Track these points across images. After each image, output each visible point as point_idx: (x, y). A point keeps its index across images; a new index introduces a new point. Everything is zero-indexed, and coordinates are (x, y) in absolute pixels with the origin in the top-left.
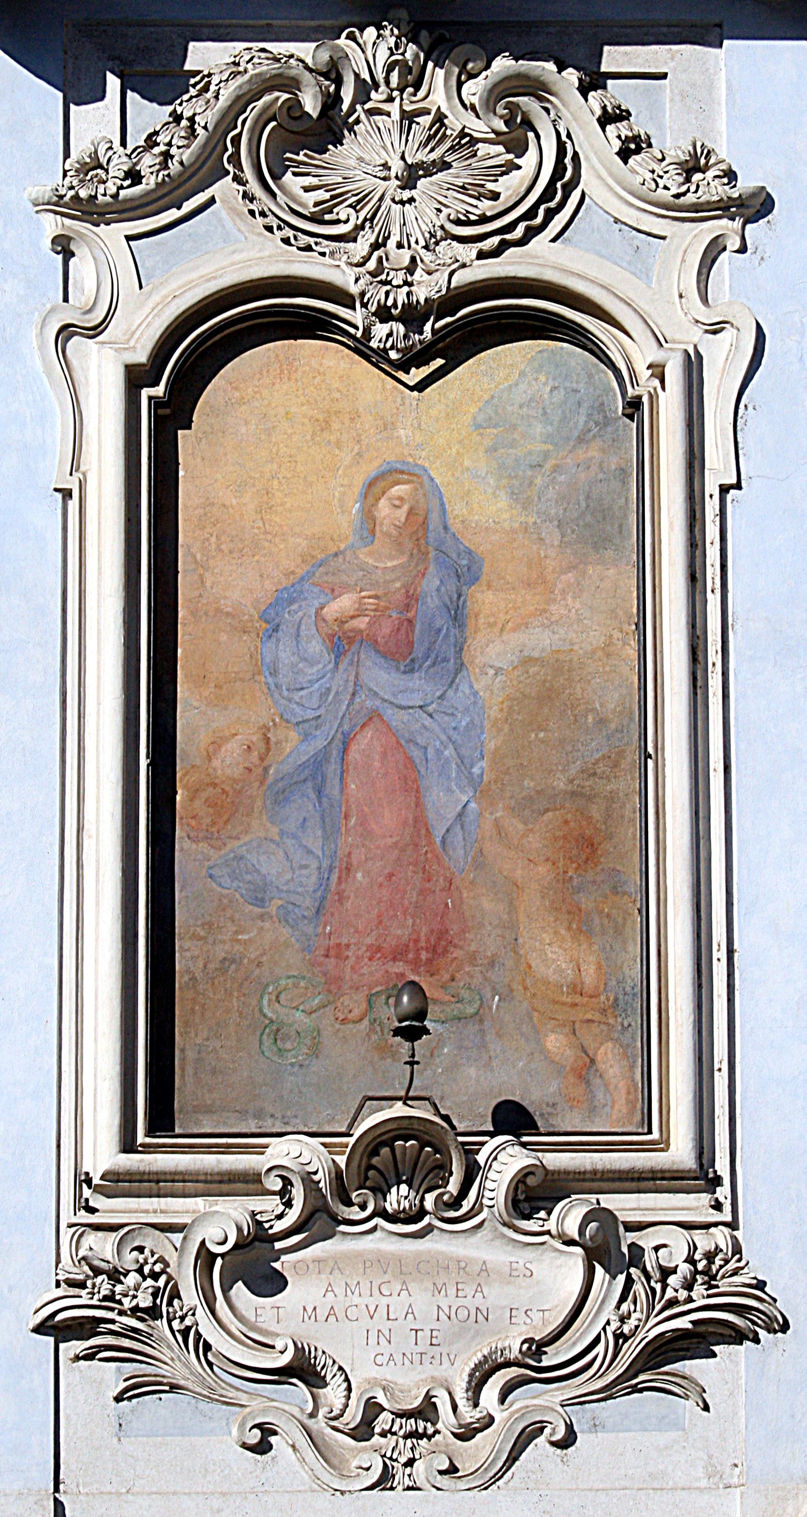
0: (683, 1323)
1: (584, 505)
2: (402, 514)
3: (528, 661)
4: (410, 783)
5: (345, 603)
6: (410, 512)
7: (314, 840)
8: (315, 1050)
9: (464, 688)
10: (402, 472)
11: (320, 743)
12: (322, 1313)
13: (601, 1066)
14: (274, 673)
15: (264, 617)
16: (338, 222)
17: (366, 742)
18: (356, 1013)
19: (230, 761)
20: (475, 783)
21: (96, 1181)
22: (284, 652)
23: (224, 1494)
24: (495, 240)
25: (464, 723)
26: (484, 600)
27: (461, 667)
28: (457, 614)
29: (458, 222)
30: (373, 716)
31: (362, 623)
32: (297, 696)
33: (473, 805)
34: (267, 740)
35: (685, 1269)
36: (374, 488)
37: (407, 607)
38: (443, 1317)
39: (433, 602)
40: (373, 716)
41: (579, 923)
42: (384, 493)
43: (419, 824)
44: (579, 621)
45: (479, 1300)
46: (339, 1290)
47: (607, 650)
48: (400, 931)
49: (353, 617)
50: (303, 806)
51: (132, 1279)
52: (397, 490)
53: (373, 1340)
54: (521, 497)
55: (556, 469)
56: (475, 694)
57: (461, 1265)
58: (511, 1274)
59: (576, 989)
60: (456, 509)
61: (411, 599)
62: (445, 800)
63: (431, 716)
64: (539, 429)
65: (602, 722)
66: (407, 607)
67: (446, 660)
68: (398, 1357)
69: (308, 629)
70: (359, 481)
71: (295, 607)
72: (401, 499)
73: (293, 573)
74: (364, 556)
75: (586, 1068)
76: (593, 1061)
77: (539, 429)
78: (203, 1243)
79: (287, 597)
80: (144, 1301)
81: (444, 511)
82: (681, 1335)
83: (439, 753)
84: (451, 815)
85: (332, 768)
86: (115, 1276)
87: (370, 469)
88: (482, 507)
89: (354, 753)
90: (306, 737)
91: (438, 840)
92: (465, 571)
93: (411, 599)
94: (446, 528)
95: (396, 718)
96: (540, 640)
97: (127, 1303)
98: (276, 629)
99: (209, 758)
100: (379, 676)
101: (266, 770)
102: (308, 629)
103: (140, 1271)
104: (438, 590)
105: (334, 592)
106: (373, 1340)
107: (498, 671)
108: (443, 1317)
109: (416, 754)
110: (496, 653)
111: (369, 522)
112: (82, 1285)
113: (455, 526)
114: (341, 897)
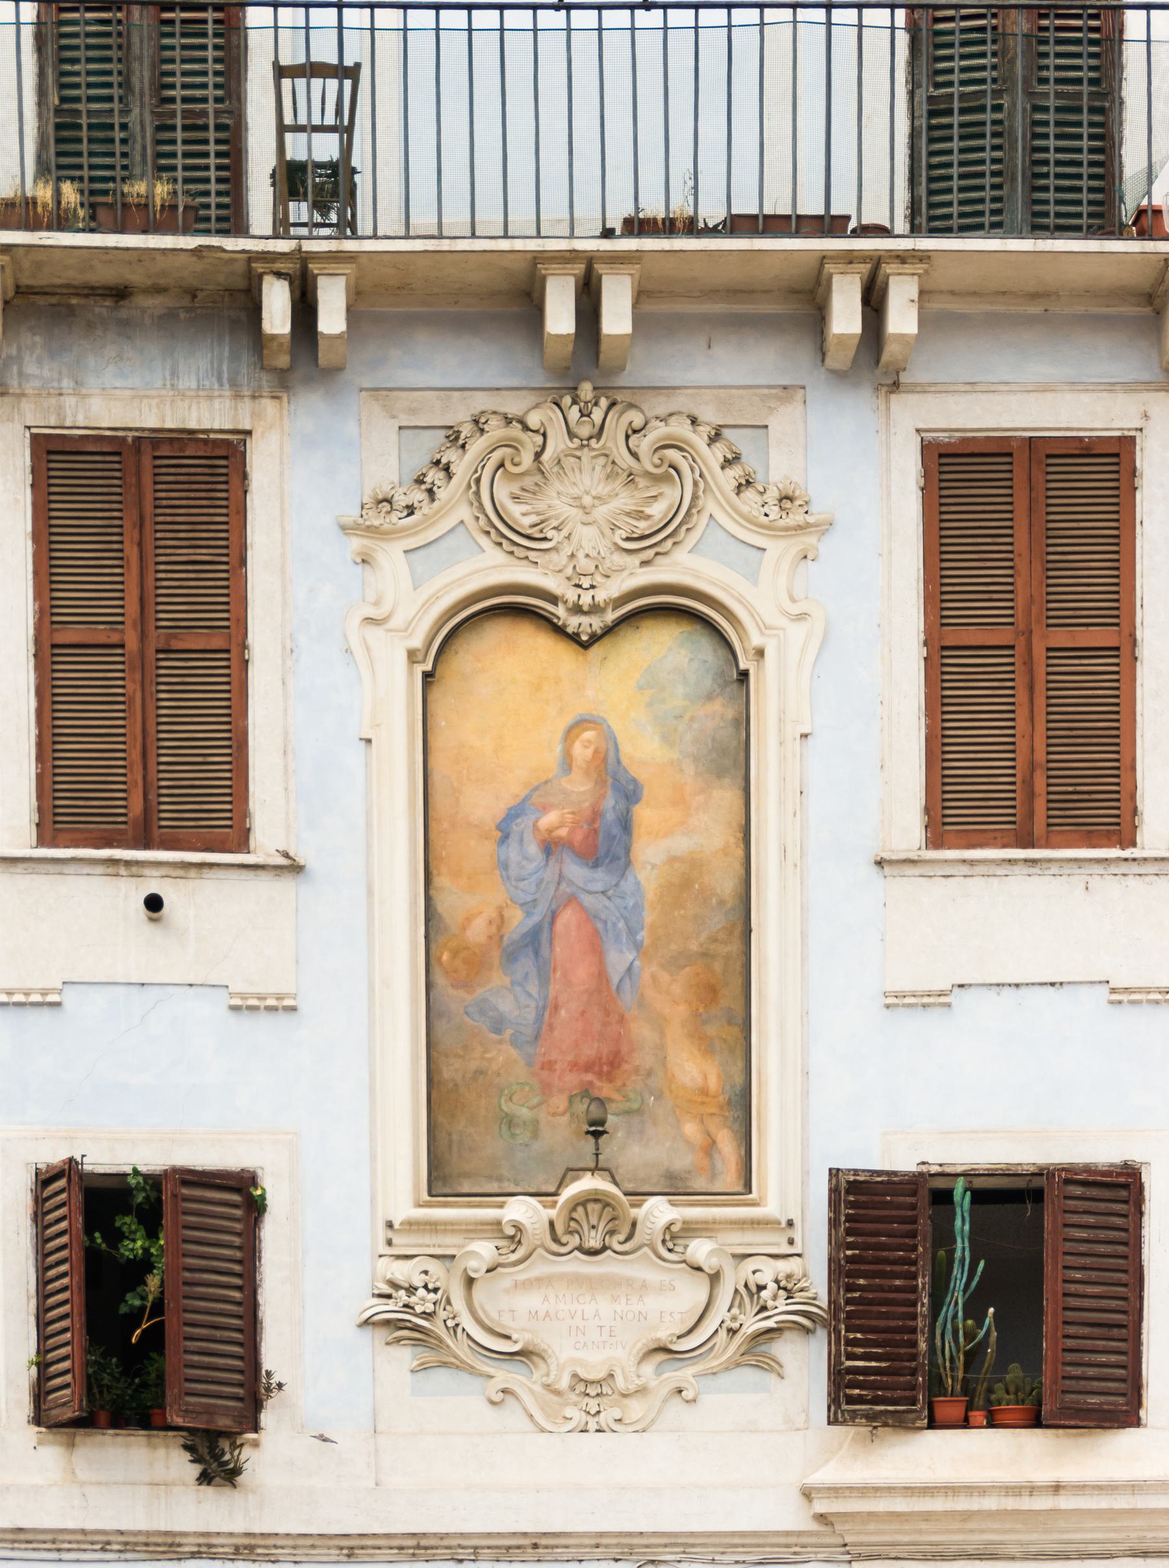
0: (770, 1323)
1: (710, 746)
2: (589, 752)
3: (672, 859)
4: (596, 948)
6: (596, 752)
7: (533, 988)
8: (535, 1135)
9: (630, 879)
10: (589, 722)
11: (536, 919)
12: (541, 1314)
13: (720, 1145)
15: (499, 828)
16: (545, 539)
17: (567, 917)
18: (561, 1109)
19: (477, 932)
20: (638, 946)
21: (396, 1226)
22: (512, 853)
24: (651, 552)
25: (631, 904)
26: (643, 814)
27: (628, 863)
28: (626, 824)
29: (628, 539)
30: (572, 899)
31: (563, 832)
32: (522, 884)
33: (637, 963)
34: (502, 917)
35: (772, 1286)
38: (618, 1317)
39: (610, 816)
40: (572, 899)
41: (707, 1046)
42: (577, 737)
43: (602, 975)
46: (552, 1299)
47: (725, 851)
48: (589, 1051)
49: (557, 828)
50: (526, 964)
51: (421, 1292)
52: (589, 735)
53: (573, 1332)
54: (667, 739)
55: (692, 719)
56: (638, 883)
57: (629, 1282)
58: (662, 1288)
59: (704, 1091)
60: (627, 749)
62: (618, 959)
63: (609, 898)
64: (680, 690)
65: (722, 903)
67: (619, 858)
69: (529, 836)
71: (519, 820)
72: (589, 741)
73: (517, 796)
74: (565, 783)
75: (710, 1147)
76: (714, 1142)
78: (465, 1270)
79: (514, 814)
80: (430, 1308)
82: (770, 1331)
83: (614, 925)
84: (622, 968)
85: (545, 936)
86: (411, 1290)
87: (569, 720)
88: (644, 748)
89: (559, 926)
90: (528, 914)
91: (614, 987)
92: (630, 793)
93: (596, 814)
94: (619, 762)
95: (587, 900)
96: (681, 844)
97: (419, 1309)
99: (464, 929)
100: (576, 871)
101: (502, 937)
102: (529, 836)
103: (426, 1287)
104: (614, 808)
105: (545, 809)
106: (573, 1332)
107: (654, 866)
108: (618, 1317)
109: (600, 926)
110: (653, 853)
112: (389, 1297)
113: (625, 761)
114: (551, 1027)
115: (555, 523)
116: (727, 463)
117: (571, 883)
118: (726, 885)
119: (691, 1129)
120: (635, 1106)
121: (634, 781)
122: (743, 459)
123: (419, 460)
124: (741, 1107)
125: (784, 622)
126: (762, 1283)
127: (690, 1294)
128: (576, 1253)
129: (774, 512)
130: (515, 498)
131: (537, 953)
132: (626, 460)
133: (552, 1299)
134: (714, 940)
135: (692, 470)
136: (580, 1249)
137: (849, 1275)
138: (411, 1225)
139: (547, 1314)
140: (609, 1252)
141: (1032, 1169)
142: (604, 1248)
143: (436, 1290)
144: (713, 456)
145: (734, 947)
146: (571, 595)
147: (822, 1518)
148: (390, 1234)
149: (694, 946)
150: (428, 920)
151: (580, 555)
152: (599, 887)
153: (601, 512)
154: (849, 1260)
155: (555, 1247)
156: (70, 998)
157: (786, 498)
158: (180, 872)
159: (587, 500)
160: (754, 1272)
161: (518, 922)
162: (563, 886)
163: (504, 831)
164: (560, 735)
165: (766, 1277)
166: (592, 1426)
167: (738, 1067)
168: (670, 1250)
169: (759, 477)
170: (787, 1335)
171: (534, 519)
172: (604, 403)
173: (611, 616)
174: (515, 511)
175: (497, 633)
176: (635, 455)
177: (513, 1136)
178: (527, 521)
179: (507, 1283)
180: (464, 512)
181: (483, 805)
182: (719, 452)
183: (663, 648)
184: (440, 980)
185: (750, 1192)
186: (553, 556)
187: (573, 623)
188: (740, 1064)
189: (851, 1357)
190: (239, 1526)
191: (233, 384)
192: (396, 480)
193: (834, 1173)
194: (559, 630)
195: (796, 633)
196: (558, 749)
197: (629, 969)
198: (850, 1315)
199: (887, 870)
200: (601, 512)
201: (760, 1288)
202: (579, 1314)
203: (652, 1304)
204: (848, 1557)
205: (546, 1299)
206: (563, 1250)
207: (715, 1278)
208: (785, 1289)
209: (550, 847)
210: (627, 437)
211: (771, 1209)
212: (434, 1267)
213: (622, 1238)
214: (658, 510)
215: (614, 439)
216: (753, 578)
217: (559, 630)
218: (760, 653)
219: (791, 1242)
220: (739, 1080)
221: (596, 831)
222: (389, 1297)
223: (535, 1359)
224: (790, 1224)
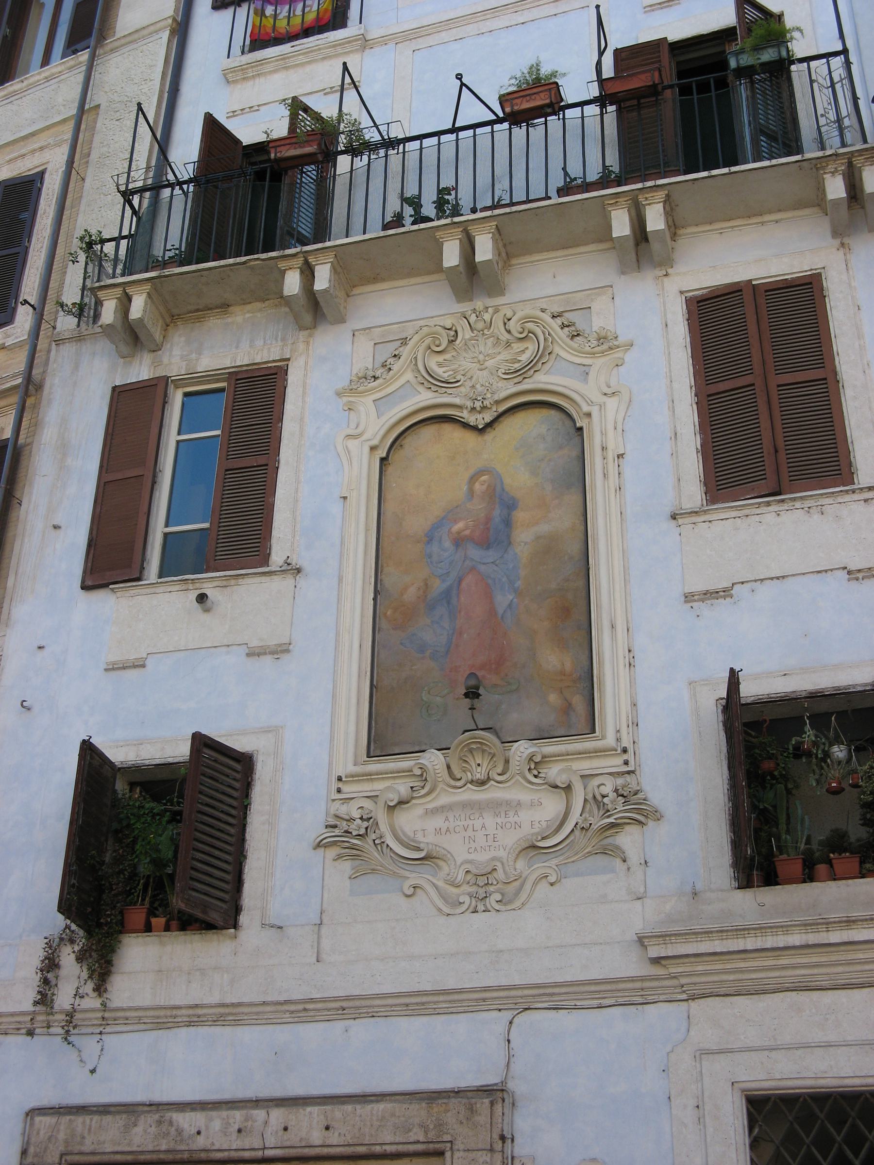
2: (484, 487)
3: (538, 538)
5: (460, 525)
6: (489, 486)
11: (448, 583)
14: (430, 556)
15: (426, 535)
17: (469, 579)
19: (411, 594)
22: (435, 548)
23: (397, 920)
26: (520, 516)
27: (510, 543)
28: (508, 523)
30: (473, 569)
31: (467, 532)
34: (426, 585)
35: (613, 795)
36: (473, 479)
38: (499, 827)
43: (492, 612)
44: (561, 519)
45: (516, 818)
51: (359, 821)
56: (516, 554)
57: (508, 803)
59: (562, 673)
60: (507, 481)
62: (502, 600)
68: (479, 849)
70: (467, 476)
72: (484, 481)
76: (570, 704)
79: (437, 526)
80: (362, 831)
81: (502, 483)
87: (472, 471)
88: (518, 478)
89: (464, 585)
91: (500, 616)
92: (510, 505)
93: (488, 519)
94: (503, 490)
95: (482, 568)
96: (544, 528)
97: (354, 834)
98: (431, 540)
99: (402, 595)
100: (474, 553)
103: (361, 818)
105: (456, 522)
107: (526, 543)
108: (499, 827)
109: (490, 581)
110: (524, 537)
111: (471, 492)
112: (335, 827)
115: (463, 373)
117: (472, 560)
118: (575, 548)
119: (553, 698)
120: (514, 687)
121: (513, 498)
122: (577, 325)
125: (605, 398)
126: (604, 793)
127: (551, 807)
128: (469, 785)
130: (440, 365)
131: (449, 603)
133: (451, 819)
135: (544, 334)
136: (471, 782)
138: (355, 778)
139: (448, 830)
140: (492, 782)
141: (804, 694)
142: (489, 779)
144: (555, 324)
145: (581, 583)
147: (656, 961)
148: (340, 785)
149: (553, 586)
150: (376, 592)
151: (478, 386)
153: (490, 363)
155: (453, 783)
157: (601, 339)
158: (225, 583)
159: (481, 357)
160: (599, 786)
161: (438, 586)
162: (467, 562)
163: (429, 538)
165: (608, 789)
166: (481, 907)
167: (584, 658)
168: (536, 776)
169: (587, 332)
170: (627, 828)
174: (440, 371)
175: (428, 432)
176: (509, 332)
178: (446, 375)
179: (420, 811)
180: (409, 376)
181: (417, 524)
182: (559, 321)
184: (384, 624)
185: (594, 732)
186: (462, 389)
187: (472, 419)
188: (587, 652)
190: (215, 998)
191: (283, 339)
192: (370, 367)
194: (466, 425)
195: (612, 404)
196: (465, 488)
197: (510, 605)
199: (680, 521)
200: (490, 363)
202: (471, 827)
203: (525, 816)
204: (684, 996)
205: (447, 819)
206: (459, 784)
207: (568, 788)
208: (622, 796)
210: (505, 324)
211: (610, 740)
212: (368, 804)
214: (525, 358)
217: (466, 425)
218: (589, 415)
219: (626, 763)
220: (586, 663)
221: (488, 529)
222: (335, 827)
223: (441, 863)
224: (625, 751)
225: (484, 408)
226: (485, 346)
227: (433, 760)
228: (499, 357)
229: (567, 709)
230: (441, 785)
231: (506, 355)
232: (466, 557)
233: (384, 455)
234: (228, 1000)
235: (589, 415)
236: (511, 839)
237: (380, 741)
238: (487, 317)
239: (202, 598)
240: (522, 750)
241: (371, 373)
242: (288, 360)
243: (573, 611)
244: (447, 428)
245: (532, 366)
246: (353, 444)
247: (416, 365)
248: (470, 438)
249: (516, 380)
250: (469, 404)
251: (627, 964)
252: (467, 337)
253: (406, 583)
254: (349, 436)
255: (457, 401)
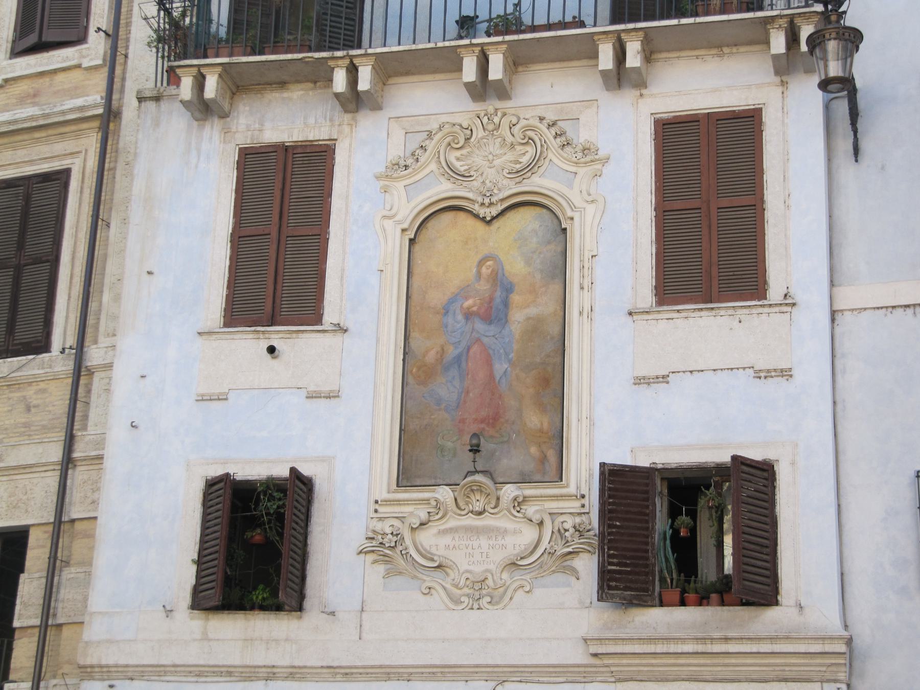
0: (570, 549)
2: (490, 271)
3: (528, 319)
4: (489, 363)
6: (493, 271)
7: (457, 383)
8: (455, 455)
11: (459, 350)
12: (451, 547)
14: (446, 327)
15: (444, 308)
17: (475, 349)
19: (431, 357)
20: (510, 361)
22: (450, 320)
26: (516, 298)
27: (507, 321)
28: (506, 304)
29: (509, 173)
30: (478, 340)
31: (475, 309)
34: (443, 350)
35: (572, 530)
36: (481, 263)
37: (490, 302)
39: (498, 300)
40: (478, 340)
41: (542, 407)
43: (491, 376)
44: (546, 306)
45: (503, 542)
46: (457, 539)
48: (483, 413)
50: (454, 372)
51: (390, 536)
52: (489, 263)
54: (528, 263)
55: (540, 253)
58: (515, 532)
59: (541, 431)
60: (507, 267)
61: (491, 299)
62: (500, 367)
64: (535, 240)
65: (552, 338)
66: (490, 302)
69: (458, 311)
75: (543, 459)
77: (535, 240)
79: (452, 300)
80: (393, 544)
82: (570, 553)
86: (385, 534)
87: (479, 257)
88: (516, 266)
89: (471, 352)
90: (456, 348)
92: (509, 289)
93: (491, 299)
96: (533, 311)
97: (387, 545)
99: (424, 357)
100: (480, 326)
102: (458, 311)
103: (392, 533)
105: (466, 298)
107: (519, 322)
109: (491, 352)
110: (518, 317)
111: (479, 273)
112: (373, 538)
113: (507, 274)
114: (465, 402)
115: (475, 168)
116: (556, 136)
117: (478, 332)
118: (556, 330)
119: (533, 450)
120: (505, 439)
121: (511, 283)
122: (568, 134)
123: (413, 145)
124: (558, 439)
125: (585, 205)
126: (567, 528)
127: (529, 534)
129: (580, 155)
130: (458, 159)
132: (510, 139)
133: (457, 539)
134: (548, 356)
136: (472, 512)
137: (610, 519)
138: (387, 502)
139: (454, 547)
141: (713, 465)
143: (397, 535)
145: (559, 359)
146: (480, 199)
147: (595, 655)
148: (377, 507)
149: (538, 360)
150: (405, 354)
151: (487, 182)
152: (492, 333)
153: (497, 162)
154: (610, 511)
155: (459, 512)
156: (231, 396)
157: (585, 150)
158: (288, 336)
159: (491, 157)
161: (451, 352)
162: (474, 334)
163: (446, 311)
164: (475, 264)
166: (476, 606)
167: (558, 420)
168: (518, 512)
169: (575, 141)
170: (581, 554)
171: (466, 167)
172: (499, 114)
173: (500, 208)
174: (458, 164)
177: (443, 456)
178: (462, 169)
179: (434, 531)
180: (433, 166)
181: (436, 298)
182: (553, 131)
183: (524, 221)
184: (410, 379)
185: (562, 481)
186: (475, 183)
187: (482, 212)
188: (560, 416)
189: (610, 564)
191: (331, 120)
192: (402, 155)
193: (603, 465)
194: (476, 216)
195: (590, 209)
196: (474, 270)
197: (505, 372)
198: (610, 541)
199: (635, 317)
200: (497, 162)
201: (566, 530)
203: (509, 540)
204: (613, 679)
205: (454, 539)
206: (463, 513)
207: (541, 524)
209: (469, 315)
211: (572, 490)
212: (397, 523)
213: (492, 506)
214: (525, 160)
215: (504, 130)
216: (570, 186)
217: (476, 216)
218: (572, 219)
219: (583, 506)
220: (558, 424)
221: (491, 308)
222: (373, 538)
223: (448, 570)
225: (491, 204)
226: (494, 147)
227: (444, 494)
228: (504, 158)
229: (543, 459)
230: (450, 513)
231: (510, 156)
232: (473, 329)
233: (412, 236)
234: (296, 664)
235: (572, 219)
236: (499, 557)
237: (406, 477)
238: (496, 120)
239: (271, 350)
240: (509, 492)
241: (402, 163)
242: (336, 140)
243: (551, 382)
244: (462, 215)
245: (531, 167)
246: (388, 224)
247: (439, 157)
248: (480, 225)
249: (518, 180)
250: (480, 199)
251: (577, 656)
252: (479, 136)
253: (428, 347)
254: (384, 217)
255: (470, 195)
